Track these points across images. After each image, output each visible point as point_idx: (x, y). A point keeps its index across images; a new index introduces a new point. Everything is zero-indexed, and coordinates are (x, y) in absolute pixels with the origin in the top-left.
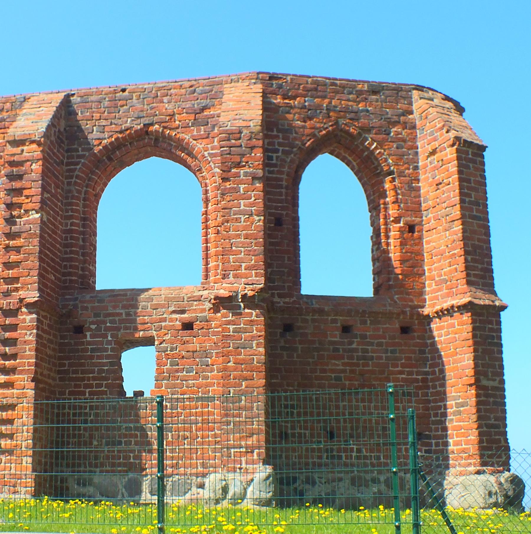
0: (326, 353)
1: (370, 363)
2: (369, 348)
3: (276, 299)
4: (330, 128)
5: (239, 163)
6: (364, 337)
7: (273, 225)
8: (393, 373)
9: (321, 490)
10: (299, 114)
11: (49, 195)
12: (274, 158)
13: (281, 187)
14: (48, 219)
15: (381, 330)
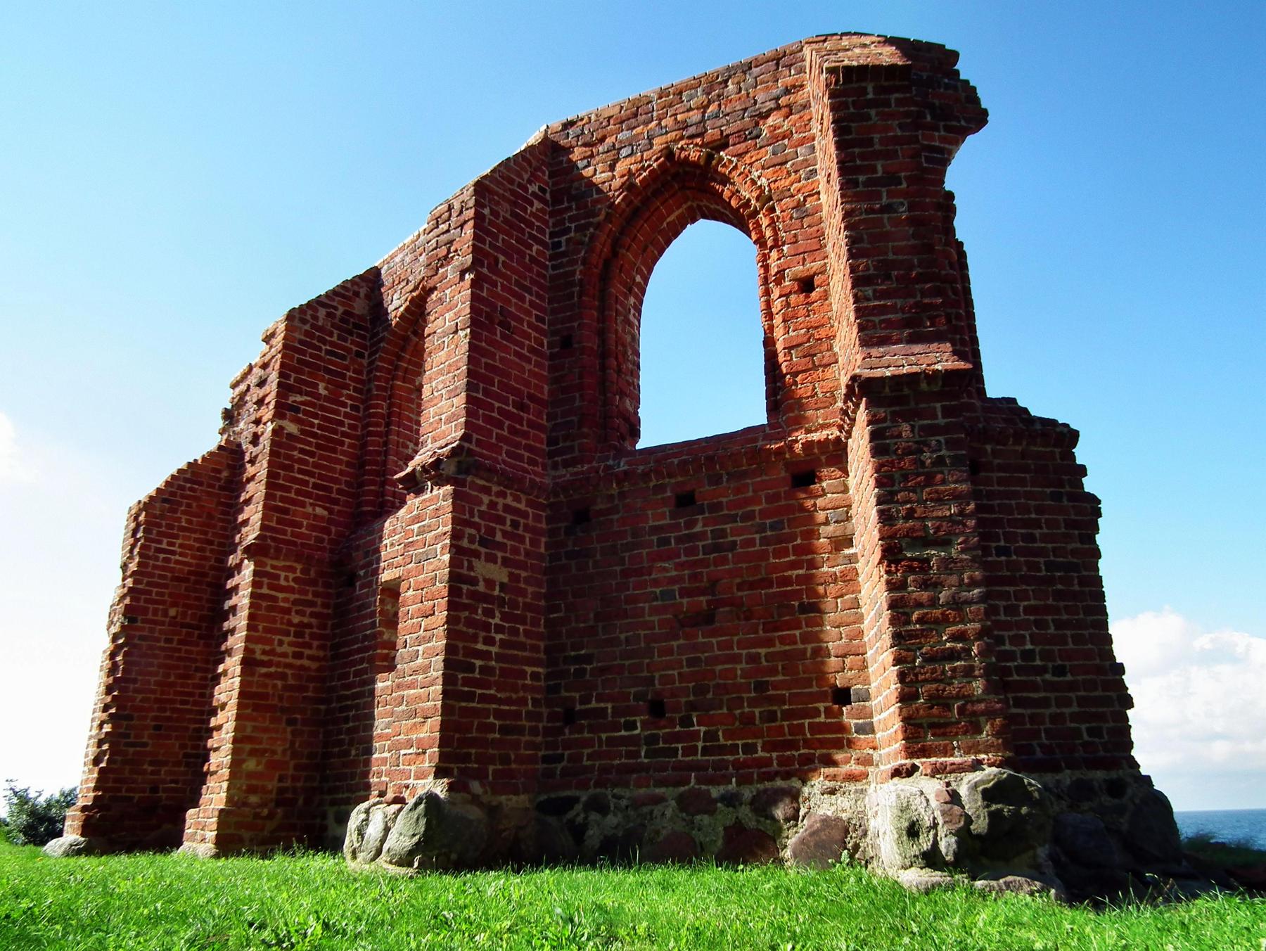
0: (645, 552)
1: (730, 555)
2: (728, 526)
3: (563, 471)
4: (655, 165)
5: (446, 257)
6: (715, 507)
7: (557, 350)
8: (776, 568)
9: (600, 827)
10: (604, 161)
11: (309, 398)
12: (564, 244)
13: (572, 284)
14: (303, 432)
15: (751, 489)
